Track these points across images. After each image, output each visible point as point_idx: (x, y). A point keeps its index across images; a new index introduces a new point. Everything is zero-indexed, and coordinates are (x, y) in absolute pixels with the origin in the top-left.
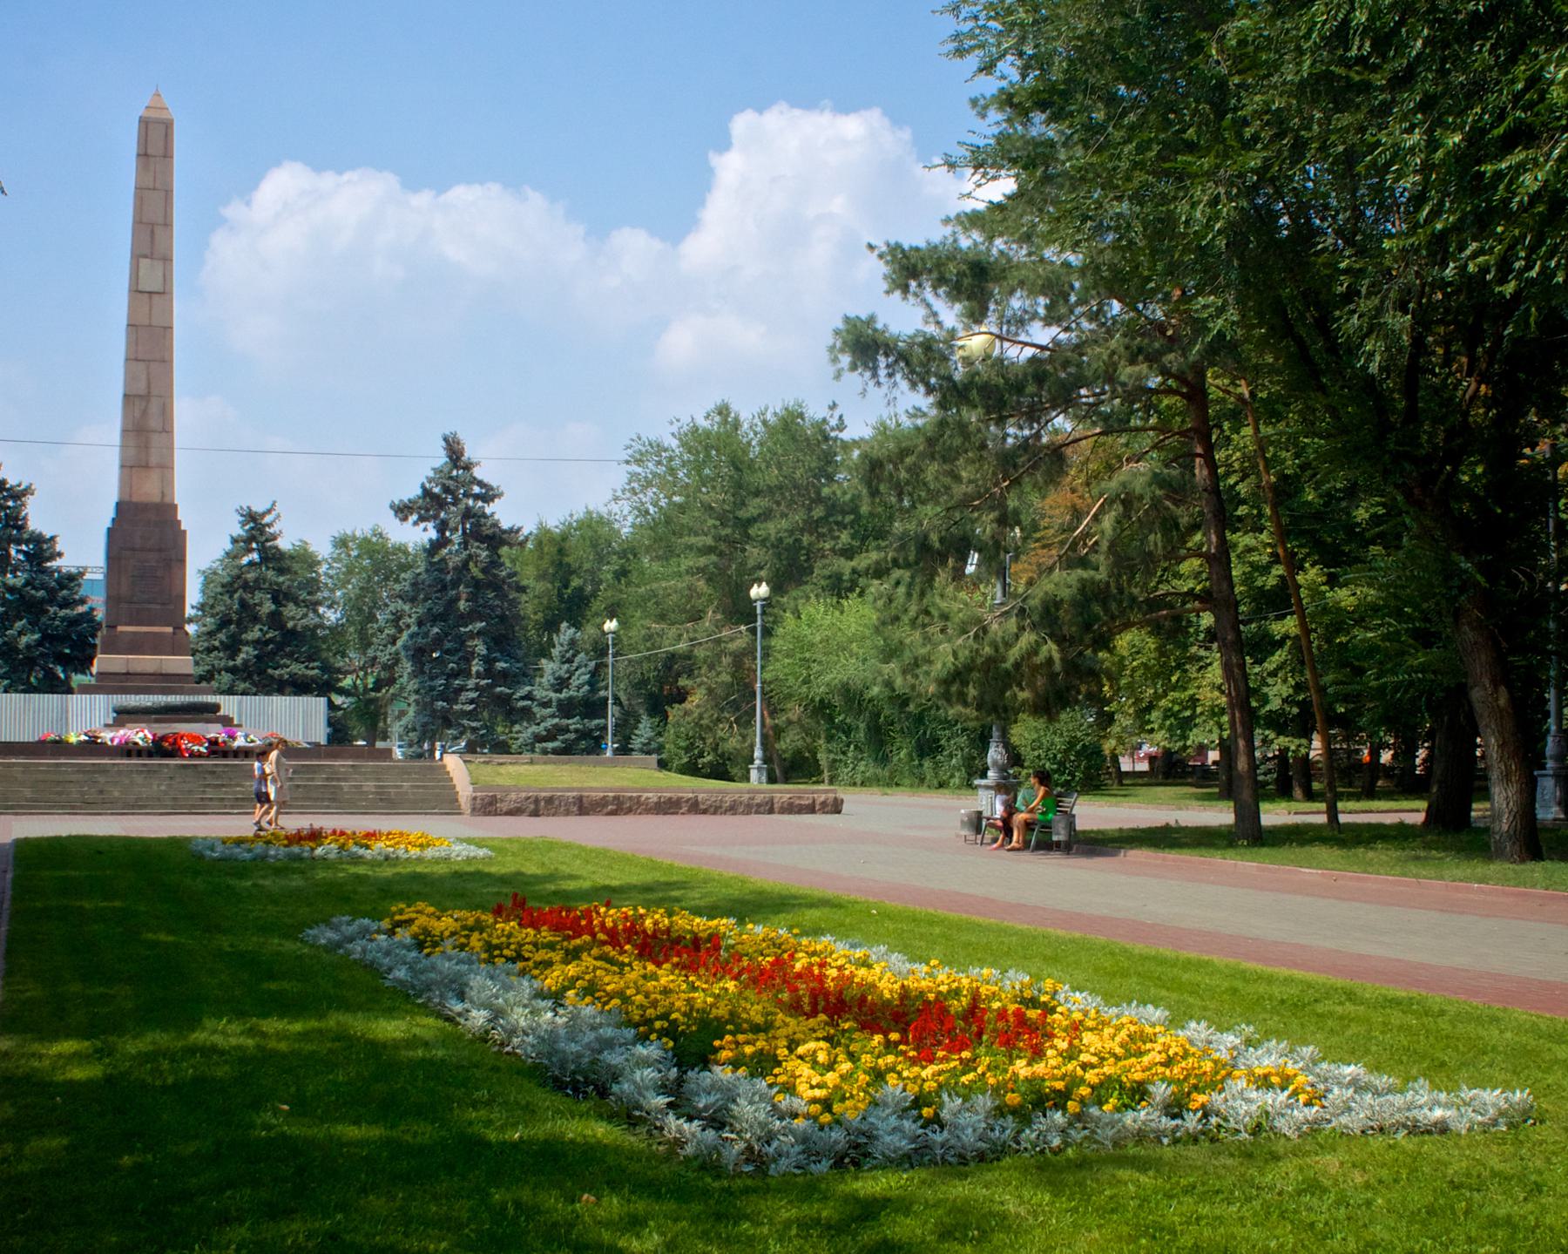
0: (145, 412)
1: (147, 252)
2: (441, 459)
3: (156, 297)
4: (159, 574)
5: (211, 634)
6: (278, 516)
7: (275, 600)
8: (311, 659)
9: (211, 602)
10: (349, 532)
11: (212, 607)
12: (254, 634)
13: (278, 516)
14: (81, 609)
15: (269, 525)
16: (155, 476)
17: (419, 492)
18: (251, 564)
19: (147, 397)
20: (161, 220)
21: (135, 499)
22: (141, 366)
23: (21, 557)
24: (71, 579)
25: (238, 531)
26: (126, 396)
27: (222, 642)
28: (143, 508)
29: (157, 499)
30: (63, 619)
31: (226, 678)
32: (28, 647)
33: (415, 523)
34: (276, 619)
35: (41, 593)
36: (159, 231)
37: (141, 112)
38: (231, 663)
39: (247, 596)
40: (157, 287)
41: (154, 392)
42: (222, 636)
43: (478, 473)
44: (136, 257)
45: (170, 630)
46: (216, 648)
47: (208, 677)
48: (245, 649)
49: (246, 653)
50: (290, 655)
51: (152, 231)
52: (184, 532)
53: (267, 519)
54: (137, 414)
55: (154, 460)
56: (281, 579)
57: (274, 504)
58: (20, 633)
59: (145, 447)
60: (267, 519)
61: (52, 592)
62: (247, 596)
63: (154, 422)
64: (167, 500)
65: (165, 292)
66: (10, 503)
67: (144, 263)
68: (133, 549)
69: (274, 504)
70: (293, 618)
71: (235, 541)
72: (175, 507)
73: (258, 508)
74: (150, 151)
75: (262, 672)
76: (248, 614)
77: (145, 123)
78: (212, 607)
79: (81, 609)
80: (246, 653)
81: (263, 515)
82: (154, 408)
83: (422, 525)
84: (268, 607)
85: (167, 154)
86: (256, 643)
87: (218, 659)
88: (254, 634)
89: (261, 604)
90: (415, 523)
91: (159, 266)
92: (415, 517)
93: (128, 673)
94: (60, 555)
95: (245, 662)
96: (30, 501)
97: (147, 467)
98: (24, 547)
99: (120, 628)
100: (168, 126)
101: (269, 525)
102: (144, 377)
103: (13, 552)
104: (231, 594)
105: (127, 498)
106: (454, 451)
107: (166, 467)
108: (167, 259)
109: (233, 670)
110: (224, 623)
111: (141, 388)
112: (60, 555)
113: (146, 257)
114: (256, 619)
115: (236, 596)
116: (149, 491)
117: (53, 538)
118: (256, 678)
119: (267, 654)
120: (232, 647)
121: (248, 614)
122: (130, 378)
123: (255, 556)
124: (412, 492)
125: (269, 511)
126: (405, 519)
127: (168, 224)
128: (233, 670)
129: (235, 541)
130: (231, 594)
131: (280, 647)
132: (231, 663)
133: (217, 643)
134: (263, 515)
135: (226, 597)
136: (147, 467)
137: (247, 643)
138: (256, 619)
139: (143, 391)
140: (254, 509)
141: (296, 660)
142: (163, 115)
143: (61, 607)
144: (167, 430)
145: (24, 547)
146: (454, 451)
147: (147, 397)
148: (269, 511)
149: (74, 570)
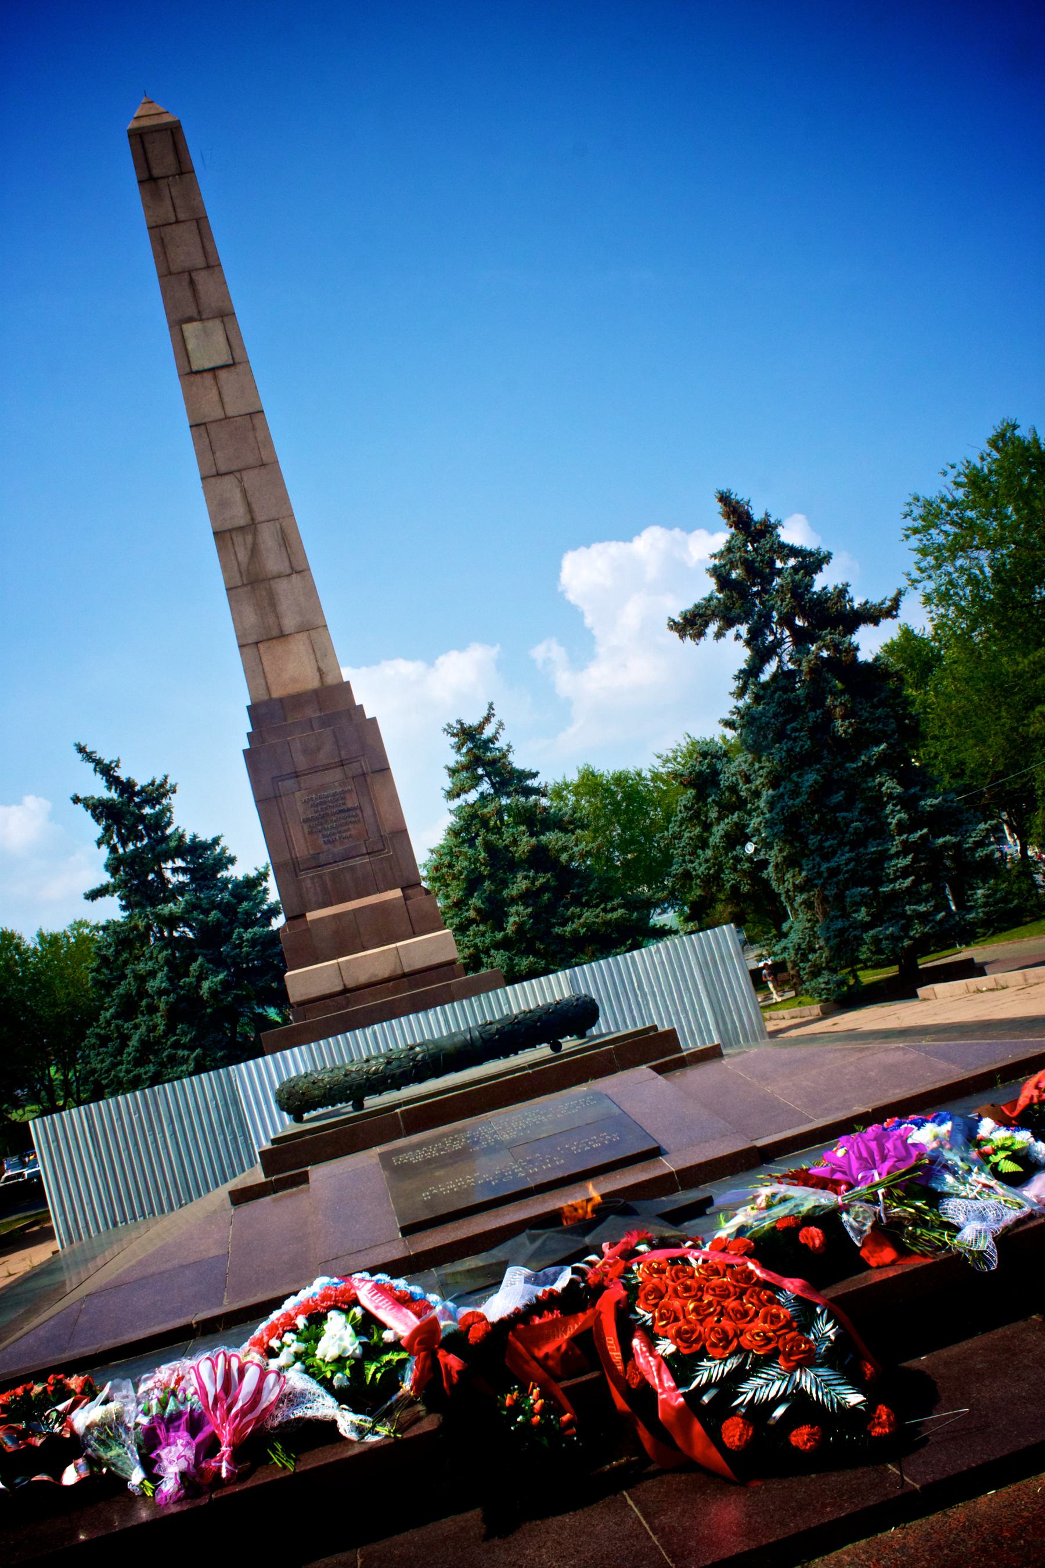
0: (254, 552)
1: (192, 311)
3: (223, 375)
4: (351, 802)
5: (459, 905)
6: (501, 725)
8: (605, 898)
9: (446, 860)
10: (560, 780)
11: (450, 866)
12: (520, 884)
13: (501, 725)
15: (492, 740)
16: (299, 645)
18: (483, 796)
19: (252, 527)
21: (276, 694)
22: (229, 484)
23: (183, 878)
25: (454, 759)
26: (215, 534)
27: (478, 911)
28: (297, 701)
29: (313, 683)
30: (254, 942)
31: (499, 957)
32: (213, 992)
33: (719, 635)
35: (214, 914)
38: (500, 935)
39: (493, 838)
41: (260, 517)
42: (475, 901)
44: (177, 324)
45: (397, 893)
46: (471, 922)
47: (474, 963)
48: (513, 910)
49: (516, 916)
50: (576, 901)
51: (192, 282)
53: (488, 732)
54: (243, 556)
55: (289, 623)
57: (491, 707)
58: (200, 978)
59: (270, 604)
60: (488, 732)
62: (493, 838)
63: (273, 562)
64: (330, 680)
66: (147, 810)
67: (189, 329)
68: (296, 775)
69: (491, 707)
70: (565, 849)
71: (453, 772)
72: (346, 687)
73: (472, 720)
74: (157, 172)
75: (546, 935)
76: (501, 861)
78: (450, 866)
80: (516, 916)
81: (481, 727)
82: (268, 537)
83: (731, 633)
86: (526, 897)
87: (482, 935)
88: (520, 884)
89: (515, 842)
90: (719, 635)
92: (713, 628)
93: (346, 990)
94: (232, 860)
95: (520, 926)
96: (174, 800)
98: (180, 863)
99: (311, 916)
102: (238, 496)
103: (168, 874)
105: (263, 696)
107: (313, 626)
108: (226, 315)
109: (504, 944)
110: (473, 884)
111: (238, 515)
112: (232, 860)
113: (190, 320)
115: (479, 841)
116: (294, 672)
117: (216, 841)
119: (545, 909)
120: (494, 913)
121: (501, 861)
122: (217, 506)
123: (485, 787)
125: (487, 719)
126: (700, 634)
128: (504, 944)
129: (453, 772)
132: (500, 935)
133: (472, 914)
134: (481, 727)
135: (465, 848)
136: (282, 636)
137: (513, 901)
138: (513, 866)
141: (587, 905)
144: (298, 569)
145: (180, 863)
148: (487, 719)
149: (253, 874)
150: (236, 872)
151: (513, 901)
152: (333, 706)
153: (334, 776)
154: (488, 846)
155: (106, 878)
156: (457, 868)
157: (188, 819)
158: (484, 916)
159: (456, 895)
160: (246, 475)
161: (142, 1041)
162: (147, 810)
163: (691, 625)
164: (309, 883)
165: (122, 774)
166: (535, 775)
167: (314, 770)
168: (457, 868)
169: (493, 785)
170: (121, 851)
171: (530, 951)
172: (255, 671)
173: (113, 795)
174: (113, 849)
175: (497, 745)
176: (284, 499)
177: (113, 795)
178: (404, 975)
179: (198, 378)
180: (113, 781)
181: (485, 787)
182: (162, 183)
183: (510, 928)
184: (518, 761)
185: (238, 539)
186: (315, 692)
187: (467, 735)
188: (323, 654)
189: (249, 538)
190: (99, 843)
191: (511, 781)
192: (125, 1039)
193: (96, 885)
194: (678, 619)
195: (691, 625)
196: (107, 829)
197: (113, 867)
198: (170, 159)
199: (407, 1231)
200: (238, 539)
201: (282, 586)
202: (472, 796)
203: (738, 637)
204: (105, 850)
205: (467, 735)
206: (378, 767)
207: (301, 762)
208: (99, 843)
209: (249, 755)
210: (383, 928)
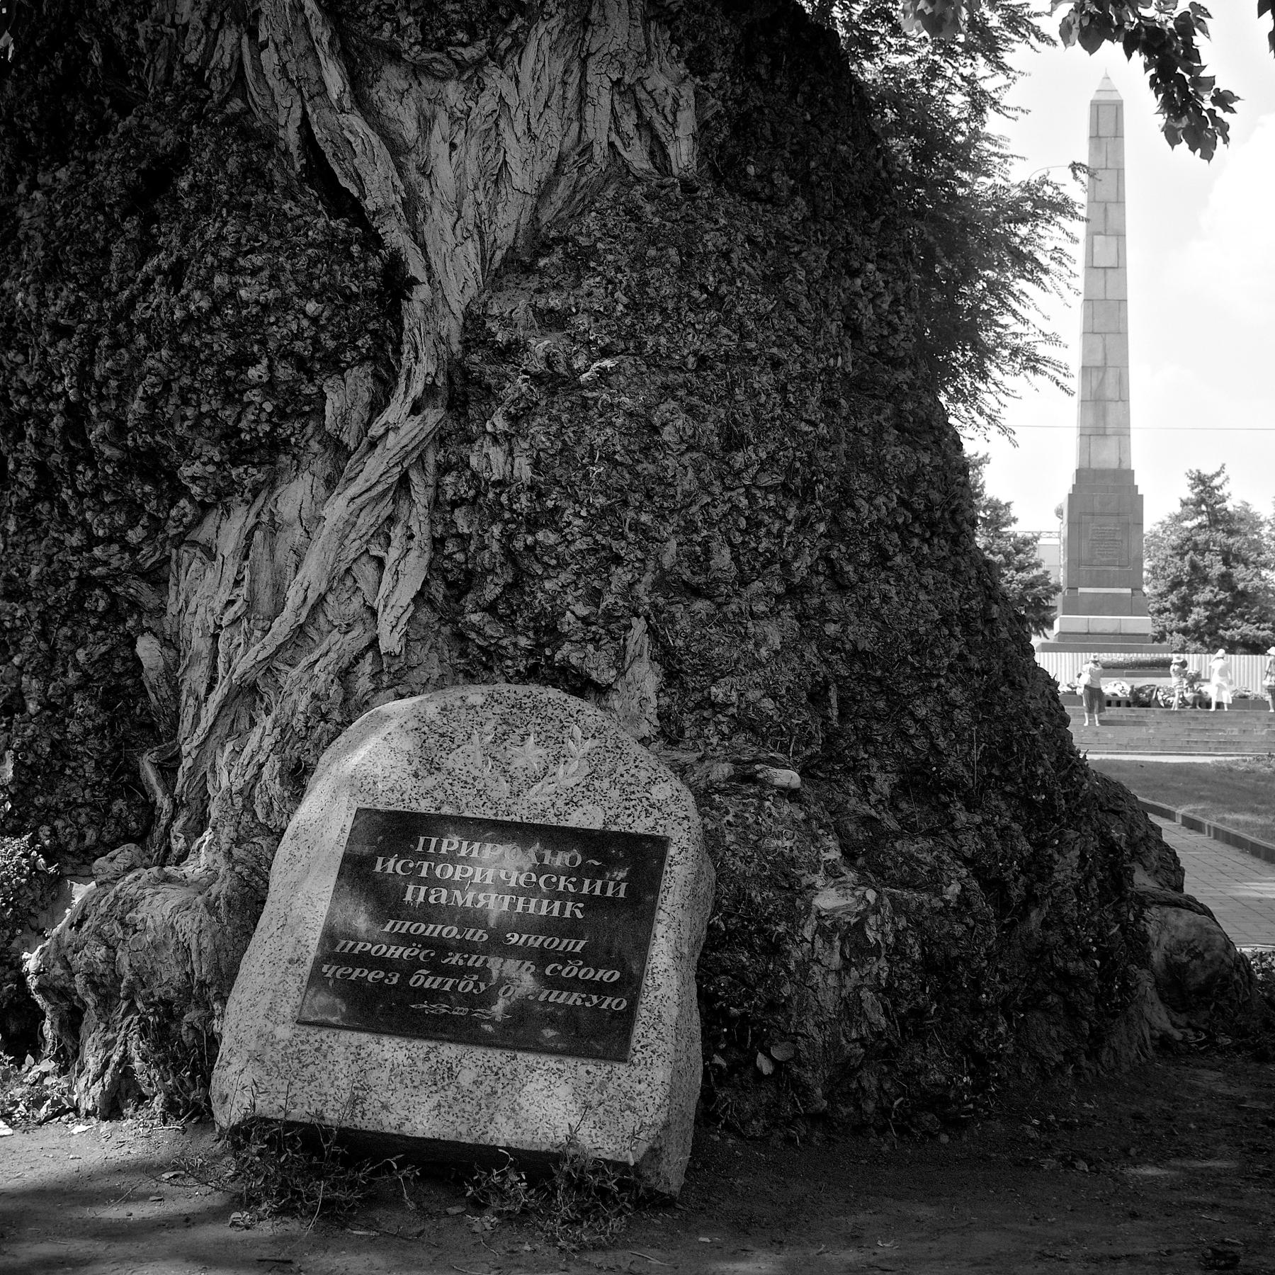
0: (1102, 383)
3: (1110, 272)
5: (1161, 595)
7: (1226, 562)
8: (1261, 619)
9: (1162, 563)
11: (1163, 569)
12: (1205, 594)
14: (1035, 572)
15: (1218, 488)
16: (1112, 442)
18: (1201, 526)
19: (1103, 368)
20: (1113, 197)
22: (1097, 339)
24: (1025, 544)
25: (1189, 494)
28: (1102, 474)
29: (1114, 465)
31: (1178, 638)
34: (1226, 581)
36: (1111, 208)
37: (1091, 96)
38: (1182, 624)
39: (1198, 558)
40: (1111, 262)
42: (1173, 597)
45: (1129, 591)
46: (1166, 610)
47: (1161, 637)
48: (1196, 610)
49: (1198, 614)
50: (1242, 616)
53: (1216, 482)
54: (1095, 384)
55: (1109, 431)
56: (1231, 541)
60: (1216, 482)
61: (1007, 555)
62: (1198, 558)
63: (1110, 392)
64: (1124, 466)
65: (1119, 267)
67: (1098, 239)
71: (1184, 504)
72: (1131, 473)
73: (1208, 471)
75: (1212, 633)
76: (1198, 576)
77: (1096, 106)
78: (1163, 569)
79: (1035, 572)
80: (1198, 614)
81: (1212, 478)
82: (1111, 376)
84: (1218, 569)
85: (1118, 134)
86: (1208, 604)
87: (1171, 621)
88: (1205, 594)
89: (1211, 566)
91: (1113, 241)
94: (1015, 520)
95: (1197, 623)
97: (1105, 435)
99: (1081, 590)
100: (1118, 107)
101: (1218, 488)
102: (1101, 349)
104: (1182, 556)
105: (1086, 465)
107: (1123, 433)
108: (1120, 235)
109: (1184, 631)
110: (1176, 584)
111: (1098, 359)
112: (1015, 520)
113: (1099, 233)
114: (1206, 580)
115: (1187, 558)
116: (1106, 457)
117: (1008, 505)
118: (1207, 639)
119: (1217, 617)
120: (1183, 608)
121: (1198, 576)
125: (1218, 474)
127: (1120, 201)
128: (1184, 631)
129: (1184, 504)
130: (1182, 556)
131: (1231, 607)
133: (1168, 605)
134: (1212, 478)
135: (1176, 560)
136: (1105, 435)
137: (1198, 604)
138: (1206, 580)
139: (1099, 364)
142: (1114, 97)
143: (1018, 570)
144: (1123, 399)
147: (1103, 368)
148: (1218, 474)
150: (1019, 529)
151: (1198, 604)
152: (1121, 481)
154: (1194, 566)
156: (1168, 571)
158: (1176, 608)
159: (1162, 589)
160: (1108, 337)
167: (1102, 514)
168: (1168, 571)
171: (1200, 638)
172: (1085, 450)
176: (1125, 357)
183: (1190, 622)
188: (1124, 449)
198: (1112, 126)
201: (1111, 406)
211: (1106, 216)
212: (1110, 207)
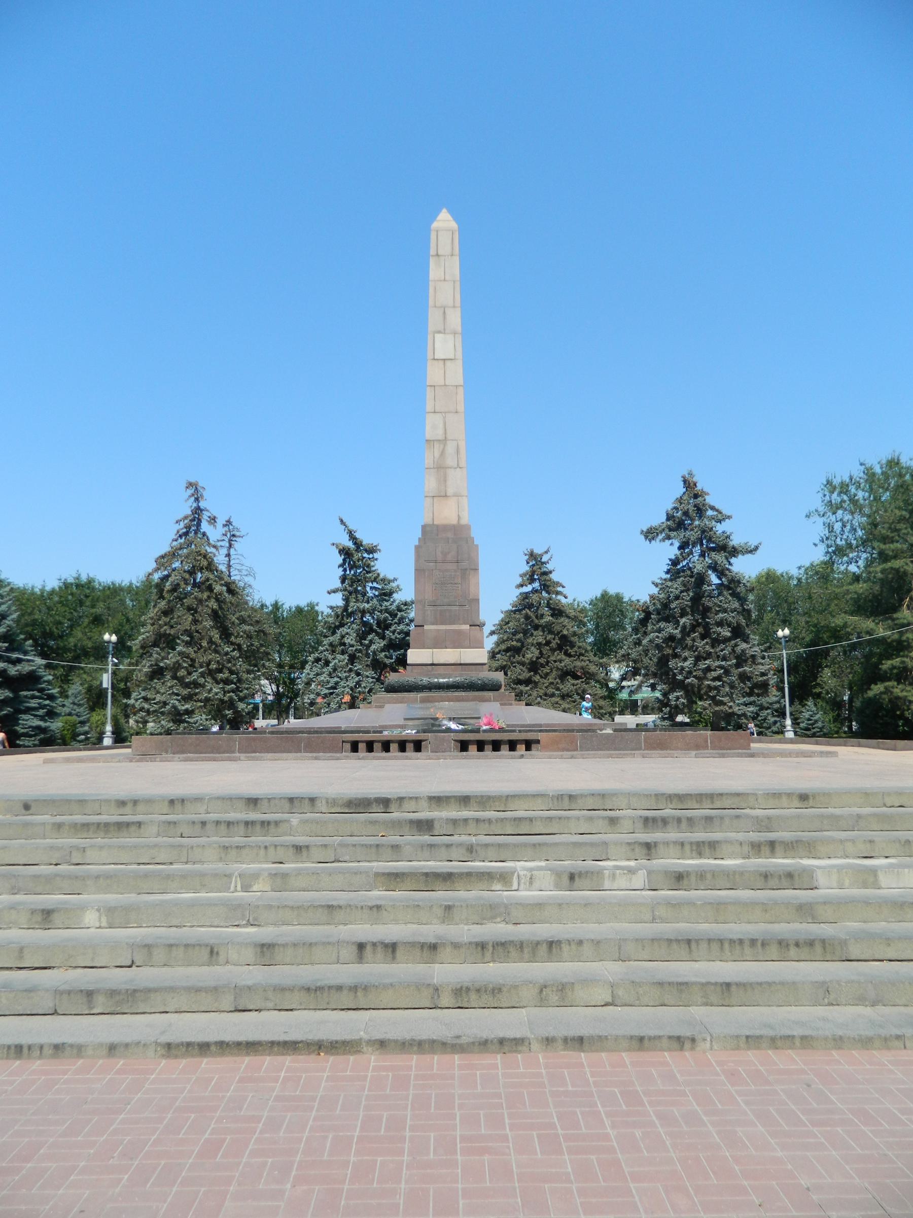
0: (443, 453)
1: (441, 328)
2: (680, 490)
3: (448, 363)
16: (452, 502)
17: (664, 518)
18: (535, 591)
19: (444, 441)
28: (445, 528)
29: (453, 521)
41: (449, 437)
43: (710, 500)
52: (477, 546)
54: (437, 454)
55: (450, 491)
60: (544, 559)
63: (450, 461)
73: (538, 551)
74: (440, 253)
82: (450, 448)
90: (663, 540)
93: (433, 665)
102: (441, 425)
103: (368, 589)
106: (689, 484)
113: (439, 332)
123: (536, 585)
124: (659, 519)
125: (546, 552)
139: (441, 437)
140: (536, 551)
146: (689, 484)
148: (546, 552)
153: (452, 567)
155: (338, 584)
157: (383, 566)
161: (335, 666)
162: (366, 555)
163: (650, 534)
164: (429, 612)
165: (357, 535)
166: (563, 587)
169: (540, 585)
170: (348, 572)
173: (350, 544)
174: (345, 570)
175: (547, 566)
177: (350, 544)
178: (461, 664)
179: (436, 362)
180: (352, 537)
181: (536, 585)
182: (442, 258)
184: (554, 577)
185: (436, 445)
186: (454, 526)
187: (532, 556)
189: (442, 446)
190: (339, 566)
191: (547, 586)
192: (327, 663)
193: (333, 587)
194: (645, 530)
195: (650, 534)
196: (344, 560)
197: (343, 579)
199: (406, 719)
200: (436, 445)
201: (451, 473)
202: (529, 588)
203: (672, 544)
204: (341, 569)
205: (532, 556)
206: (473, 567)
207: (440, 557)
208: (339, 566)
209: (417, 548)
210: (458, 641)
211: (445, 318)
212: (448, 311)
